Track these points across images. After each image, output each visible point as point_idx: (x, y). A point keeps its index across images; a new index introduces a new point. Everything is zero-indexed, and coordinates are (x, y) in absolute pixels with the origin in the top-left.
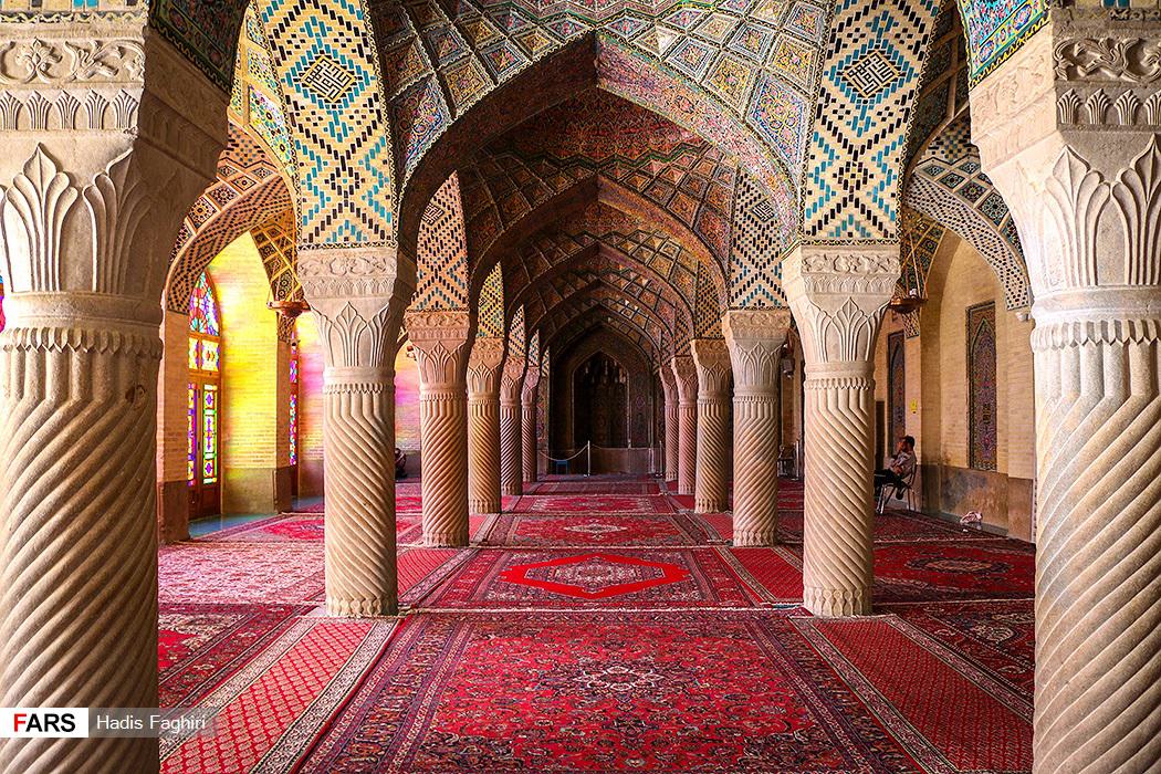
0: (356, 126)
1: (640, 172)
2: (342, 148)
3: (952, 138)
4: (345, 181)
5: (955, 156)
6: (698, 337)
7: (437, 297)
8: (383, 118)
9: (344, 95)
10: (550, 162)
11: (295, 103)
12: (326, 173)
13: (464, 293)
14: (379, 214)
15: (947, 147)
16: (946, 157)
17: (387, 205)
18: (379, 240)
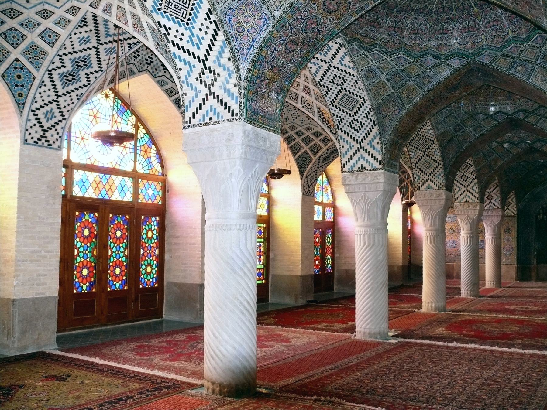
0: (204, 35)
1: (504, 55)
2: (201, 53)
4: (208, 77)
7: (362, 162)
8: (220, 26)
9: (190, 14)
10: (436, 57)
11: (165, 26)
13: (379, 157)
14: (230, 98)
17: (235, 91)
18: (231, 118)
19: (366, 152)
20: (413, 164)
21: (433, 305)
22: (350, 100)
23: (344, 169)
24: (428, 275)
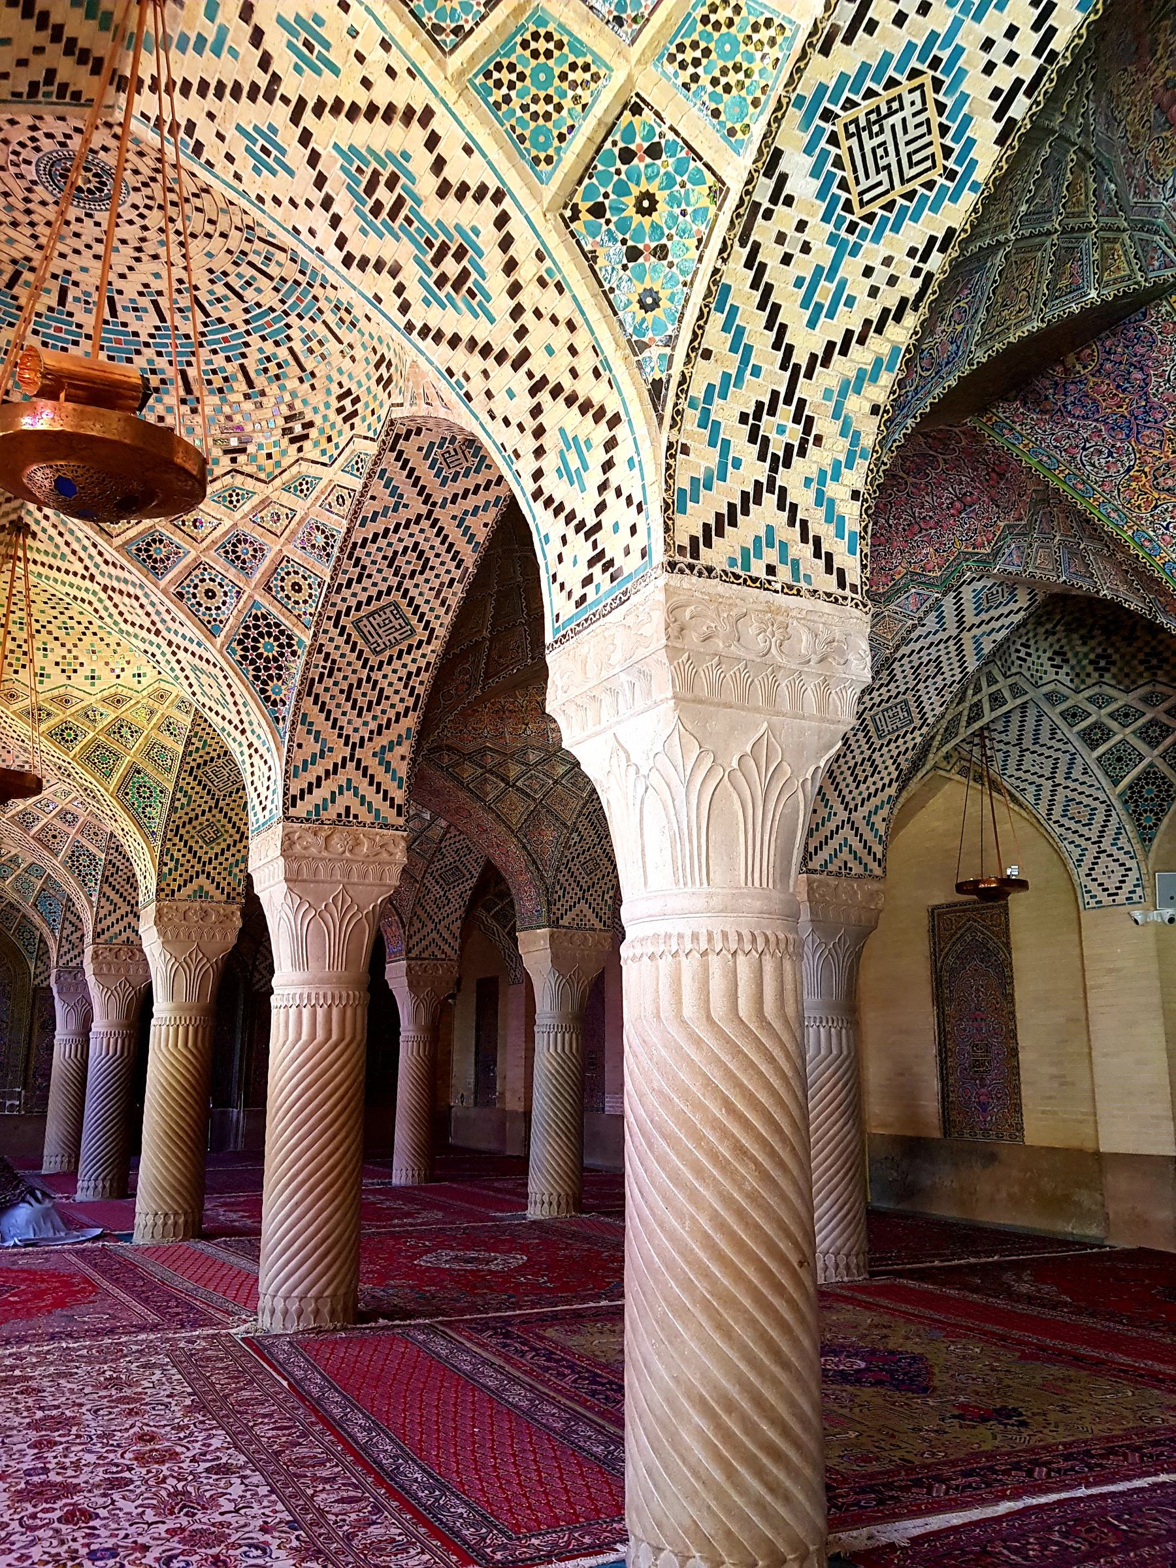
0: (862, 297)
2: (806, 342)
3: (1080, 656)
4: (781, 429)
5: (1083, 682)
6: (554, 924)
7: (347, 799)
8: (929, 297)
9: (889, 207)
12: (746, 397)
13: (399, 796)
14: (832, 529)
15: (1072, 668)
16: (1072, 681)
17: (851, 511)
18: (833, 587)
19: (364, 775)
20: (172, 826)
21: (181, 1220)
22: (395, 623)
23: (292, 812)
24: (174, 1137)
